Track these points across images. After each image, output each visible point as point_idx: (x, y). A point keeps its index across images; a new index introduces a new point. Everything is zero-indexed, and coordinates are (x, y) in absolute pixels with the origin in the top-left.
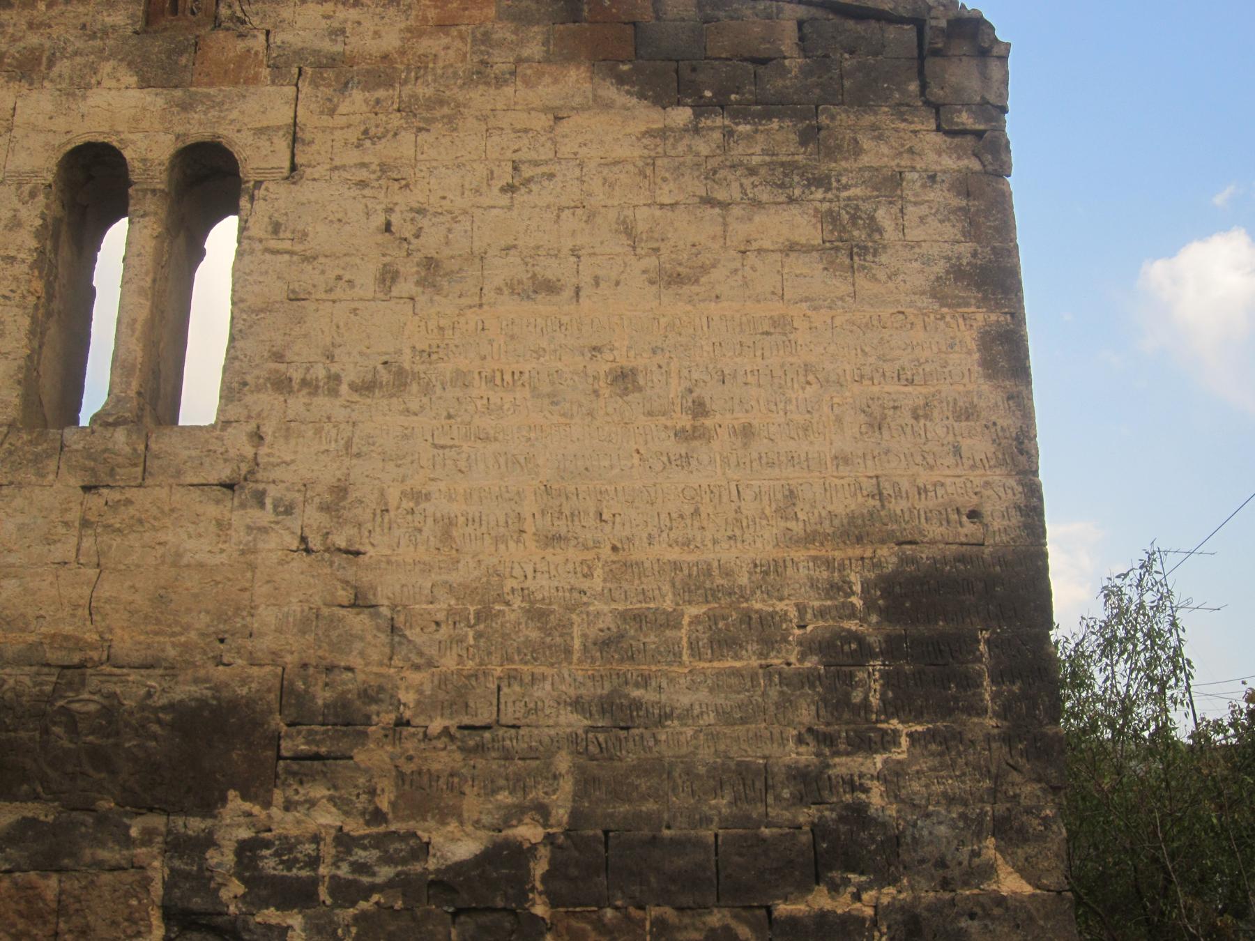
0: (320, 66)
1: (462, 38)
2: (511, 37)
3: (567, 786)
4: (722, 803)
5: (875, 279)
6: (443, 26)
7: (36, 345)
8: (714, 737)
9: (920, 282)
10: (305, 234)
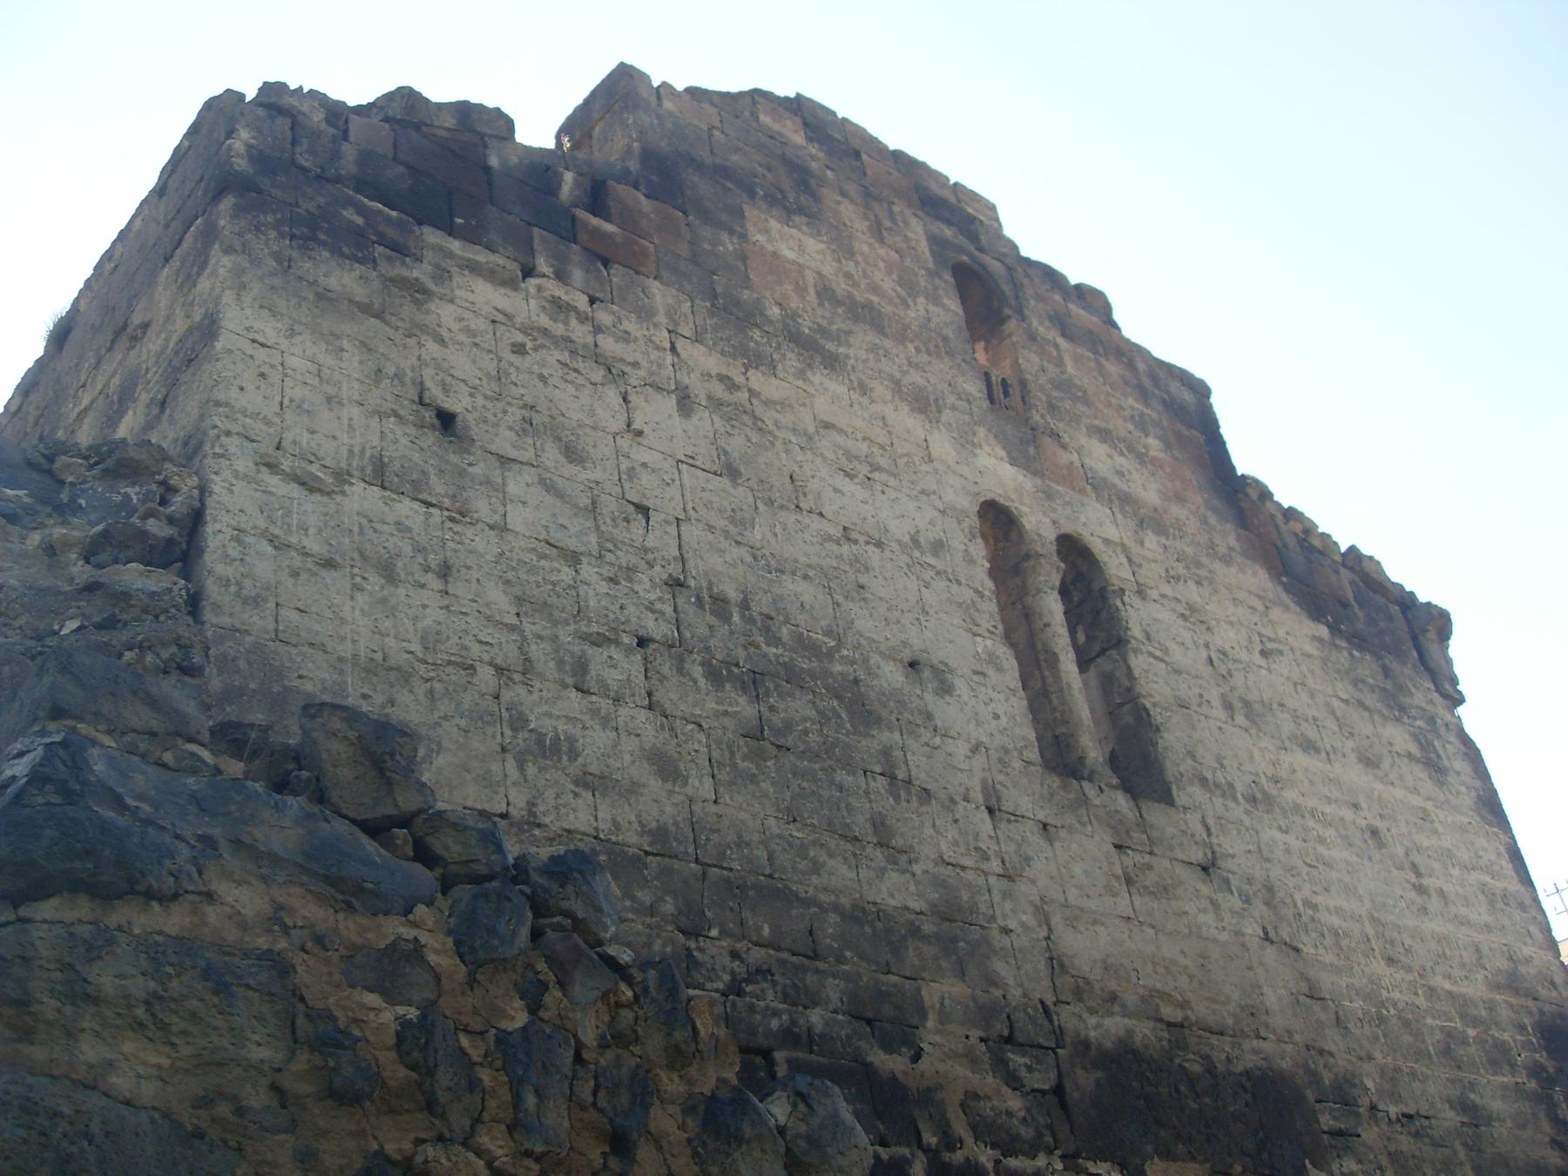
6: (1180, 499)
10: (1166, 650)
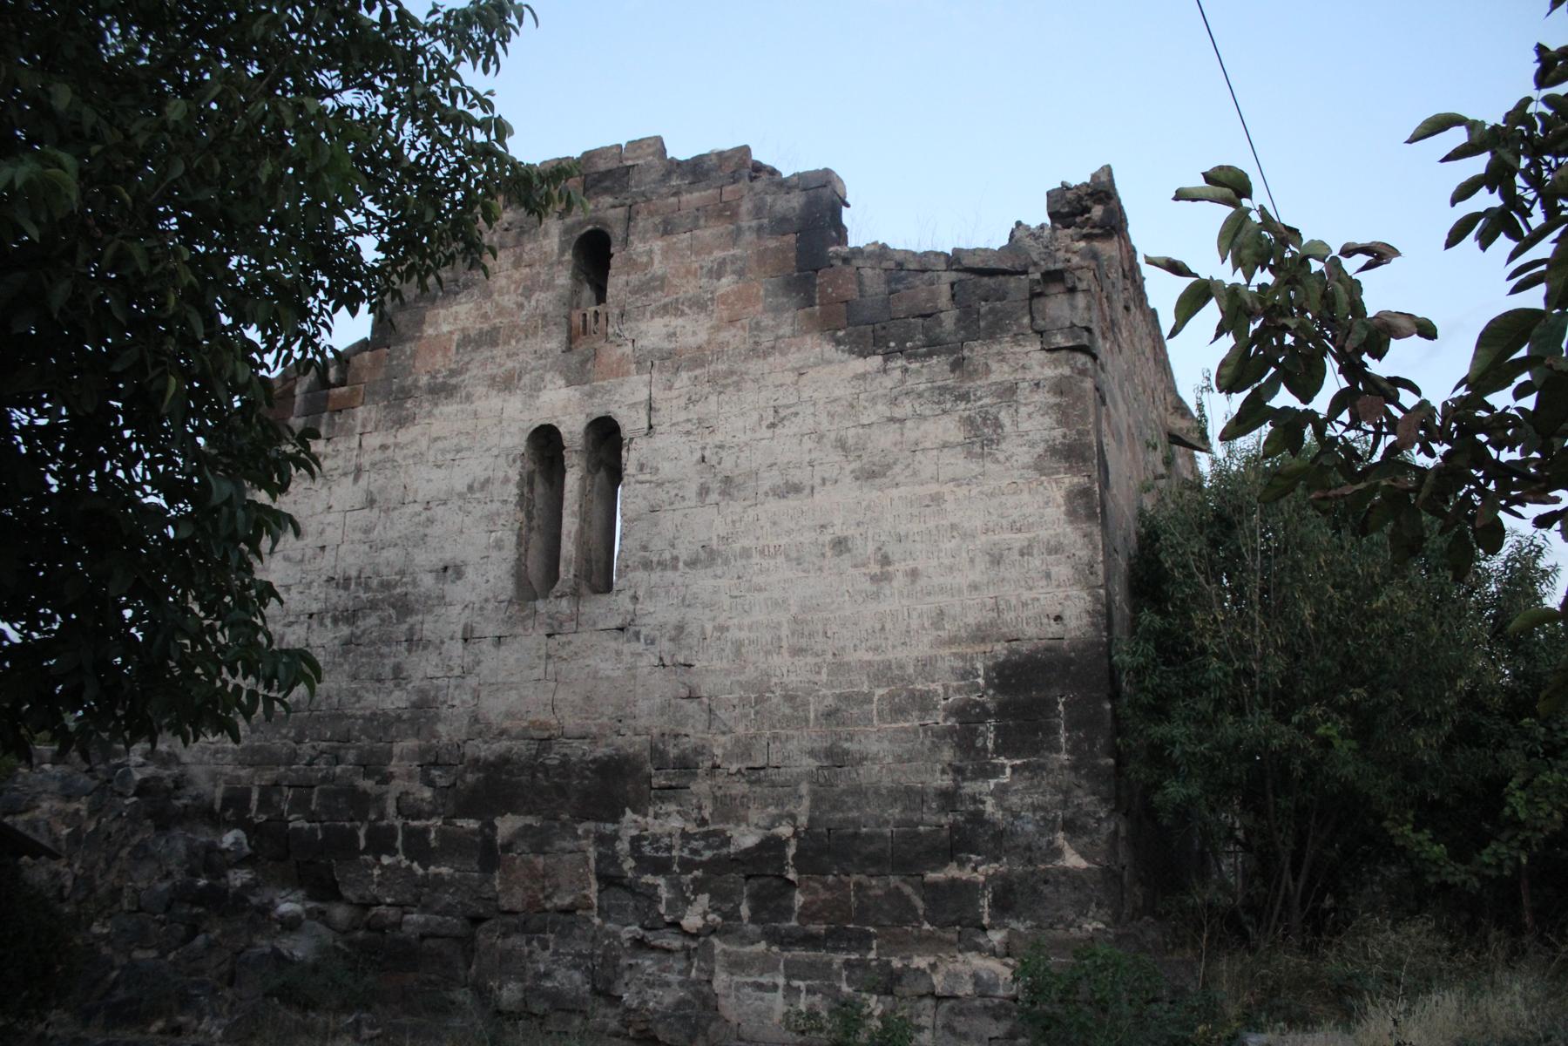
0: (662, 359)
1: (743, 328)
2: (772, 323)
3: (806, 802)
4: (896, 812)
5: (997, 461)
6: (731, 322)
7: (522, 550)
8: (891, 771)
9: (1027, 459)
